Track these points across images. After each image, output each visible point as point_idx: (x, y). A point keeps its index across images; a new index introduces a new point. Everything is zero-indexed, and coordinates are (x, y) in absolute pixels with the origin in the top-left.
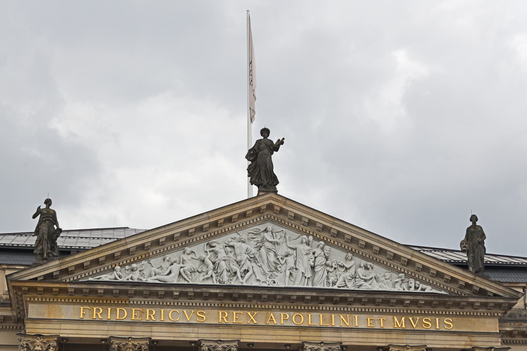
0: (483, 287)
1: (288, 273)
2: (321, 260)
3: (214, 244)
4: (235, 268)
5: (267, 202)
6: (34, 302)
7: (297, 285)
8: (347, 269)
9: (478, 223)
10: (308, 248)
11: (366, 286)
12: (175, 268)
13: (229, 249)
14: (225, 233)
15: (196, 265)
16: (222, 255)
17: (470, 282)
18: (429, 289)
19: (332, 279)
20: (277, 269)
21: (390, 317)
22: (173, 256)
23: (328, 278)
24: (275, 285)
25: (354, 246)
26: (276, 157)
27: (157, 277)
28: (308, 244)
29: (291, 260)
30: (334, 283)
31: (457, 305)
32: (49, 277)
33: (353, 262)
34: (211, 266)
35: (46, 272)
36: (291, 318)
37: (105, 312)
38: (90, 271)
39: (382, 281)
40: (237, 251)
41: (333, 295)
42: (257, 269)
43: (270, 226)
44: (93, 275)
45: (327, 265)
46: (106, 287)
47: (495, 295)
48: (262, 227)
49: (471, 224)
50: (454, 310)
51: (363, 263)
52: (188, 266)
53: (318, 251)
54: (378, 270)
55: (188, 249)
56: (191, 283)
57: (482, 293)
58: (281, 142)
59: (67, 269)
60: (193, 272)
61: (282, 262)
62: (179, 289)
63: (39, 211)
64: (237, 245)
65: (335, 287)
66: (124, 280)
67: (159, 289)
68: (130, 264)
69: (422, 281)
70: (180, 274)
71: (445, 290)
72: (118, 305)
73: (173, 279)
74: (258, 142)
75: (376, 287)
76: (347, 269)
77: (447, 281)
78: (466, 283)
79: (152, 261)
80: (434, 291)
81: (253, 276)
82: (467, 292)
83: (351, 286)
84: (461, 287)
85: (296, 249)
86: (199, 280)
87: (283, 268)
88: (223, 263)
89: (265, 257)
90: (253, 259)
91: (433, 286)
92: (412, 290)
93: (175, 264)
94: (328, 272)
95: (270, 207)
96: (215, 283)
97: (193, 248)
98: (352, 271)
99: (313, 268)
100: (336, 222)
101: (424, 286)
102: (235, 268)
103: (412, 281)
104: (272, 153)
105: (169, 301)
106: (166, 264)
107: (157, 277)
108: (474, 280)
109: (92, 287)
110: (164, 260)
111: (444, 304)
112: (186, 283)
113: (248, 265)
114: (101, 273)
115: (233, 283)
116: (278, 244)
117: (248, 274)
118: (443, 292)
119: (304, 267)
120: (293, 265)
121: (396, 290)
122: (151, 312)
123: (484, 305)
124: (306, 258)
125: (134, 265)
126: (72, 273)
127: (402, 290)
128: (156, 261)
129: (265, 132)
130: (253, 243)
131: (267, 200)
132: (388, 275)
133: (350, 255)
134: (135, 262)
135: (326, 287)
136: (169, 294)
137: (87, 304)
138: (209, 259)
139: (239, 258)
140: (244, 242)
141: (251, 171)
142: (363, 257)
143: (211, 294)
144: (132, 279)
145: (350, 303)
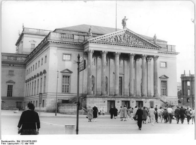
2: (133, 40)
4: (120, 40)
19: (134, 43)
30: (135, 44)
40: (121, 37)
47: (158, 48)
57: (156, 47)
64: (121, 37)
70: (112, 41)
89: (125, 39)
90: (123, 39)
99: (132, 41)
102: (120, 40)
117: (122, 42)
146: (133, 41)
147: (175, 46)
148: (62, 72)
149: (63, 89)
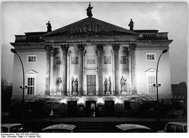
23: (101, 33)
49: (131, 21)
147: (168, 33)
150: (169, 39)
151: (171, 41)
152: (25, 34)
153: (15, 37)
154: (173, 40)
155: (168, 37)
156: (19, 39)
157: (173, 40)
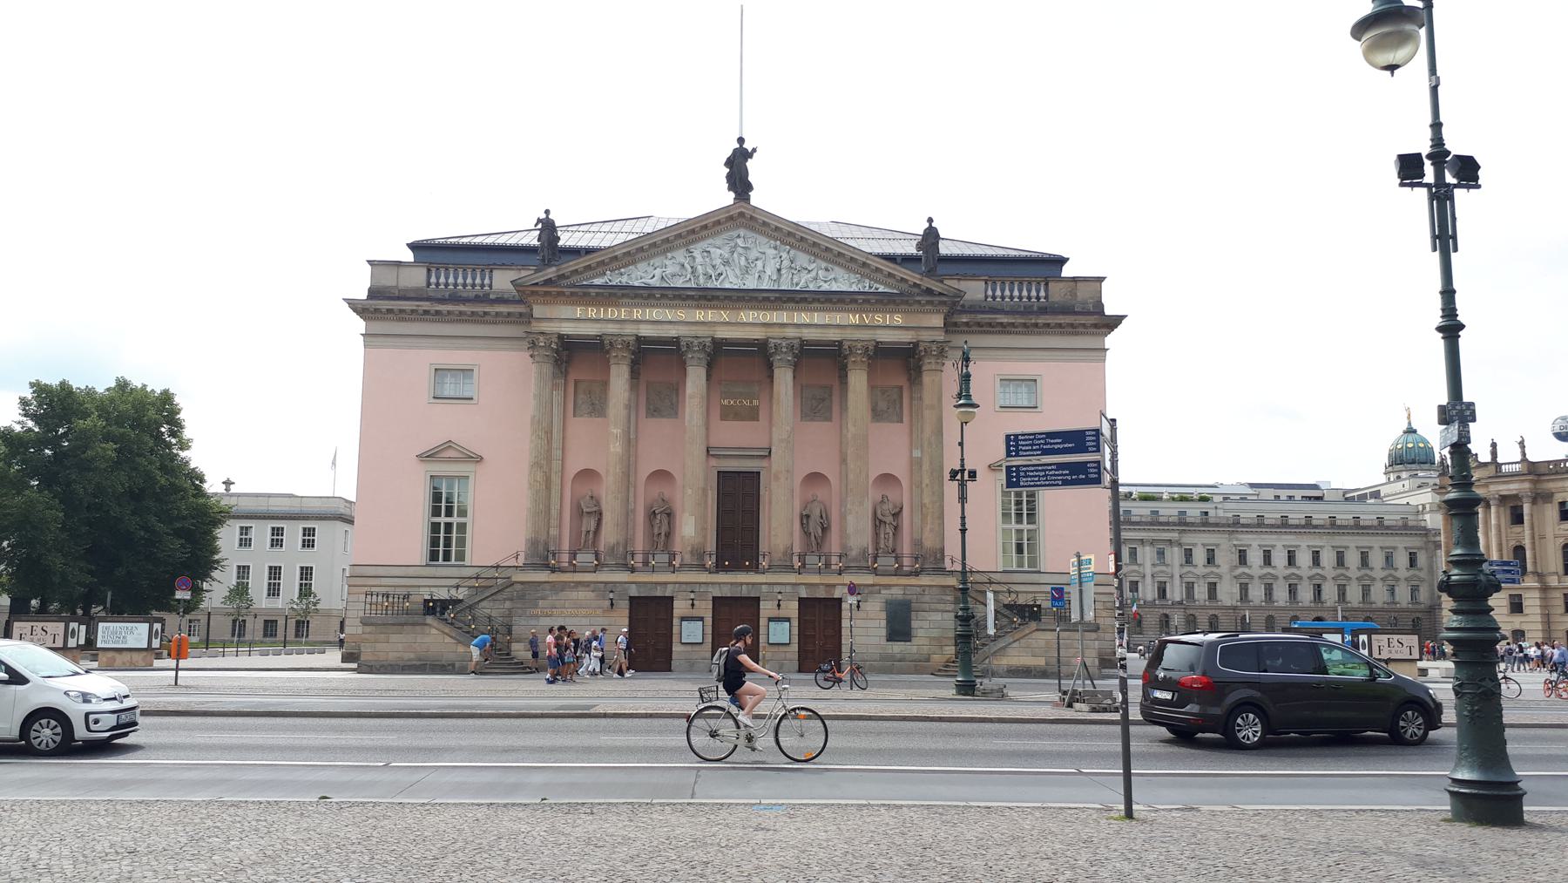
0: (929, 286)
1: (757, 275)
2: (786, 263)
3: (692, 250)
4: (710, 271)
5: (738, 211)
6: (537, 304)
7: (764, 287)
8: (809, 271)
9: (933, 225)
10: (774, 252)
11: (825, 287)
12: (658, 272)
13: (705, 254)
14: (703, 239)
15: (677, 269)
16: (699, 259)
17: (918, 282)
18: (882, 289)
20: (747, 272)
21: (846, 315)
22: (657, 261)
23: (792, 279)
24: (745, 287)
25: (815, 250)
26: (750, 164)
27: (643, 280)
28: (775, 248)
29: (759, 263)
30: (797, 285)
31: (906, 303)
32: (548, 282)
33: (815, 265)
34: (690, 270)
35: (546, 278)
36: (758, 316)
37: (598, 312)
38: (585, 275)
39: (841, 282)
40: (713, 256)
41: (793, 296)
42: (730, 272)
43: (742, 232)
44: (587, 279)
45: (792, 268)
46: (597, 290)
47: (940, 294)
48: (735, 234)
50: (903, 307)
51: (824, 265)
52: (669, 270)
53: (784, 255)
54: (839, 272)
55: (669, 255)
56: (672, 285)
57: (929, 292)
58: (754, 150)
59: (563, 275)
60: (673, 276)
61: (753, 265)
62: (660, 292)
63: (539, 220)
64: (712, 250)
65: (798, 288)
66: (614, 284)
67: (642, 292)
68: (621, 268)
69: (876, 281)
71: (898, 289)
72: (609, 306)
73: (655, 282)
74: (735, 150)
75: (835, 287)
76: (809, 271)
77: (897, 281)
78: (915, 283)
79: (639, 265)
80: (886, 290)
81: (727, 279)
82: (916, 290)
83: (812, 287)
84: (910, 286)
85: (764, 253)
86: (679, 283)
87: (753, 271)
88: (699, 267)
90: (726, 263)
91: (885, 284)
92: (867, 289)
93: (658, 269)
94: (793, 274)
95: (741, 214)
96: (693, 286)
97: (675, 254)
98: (813, 274)
99: (779, 270)
100: (800, 228)
101: (878, 286)
103: (867, 281)
104: (747, 161)
105: (653, 302)
106: (650, 269)
107: (643, 280)
108: (921, 280)
109: (585, 290)
110: (649, 264)
111: (894, 302)
112: (668, 285)
113: (721, 269)
114: (594, 277)
115: (709, 286)
116: (749, 249)
117: (722, 277)
118: (895, 291)
119: (770, 270)
120: (762, 269)
121: (852, 290)
122: (638, 312)
123: (928, 302)
124: (773, 261)
125: (623, 270)
126: (568, 278)
127: (857, 290)
128: (642, 266)
129: (741, 140)
130: (727, 248)
131: (742, 208)
132: (846, 276)
133: (813, 258)
134: (623, 267)
135: (790, 288)
136: (651, 296)
137: (583, 305)
138: (688, 263)
139: (714, 263)
140: (719, 248)
141: (730, 178)
142: (824, 259)
143: (687, 296)
144: (620, 282)
145: (810, 303)
146: (783, 272)
147: (1101, 280)
148: (429, 456)
149: (434, 542)
150: (1108, 312)
151: (1115, 322)
152: (408, 256)
153: (370, 267)
154: (1124, 317)
155: (1103, 301)
156: (389, 280)
157: (1124, 317)
